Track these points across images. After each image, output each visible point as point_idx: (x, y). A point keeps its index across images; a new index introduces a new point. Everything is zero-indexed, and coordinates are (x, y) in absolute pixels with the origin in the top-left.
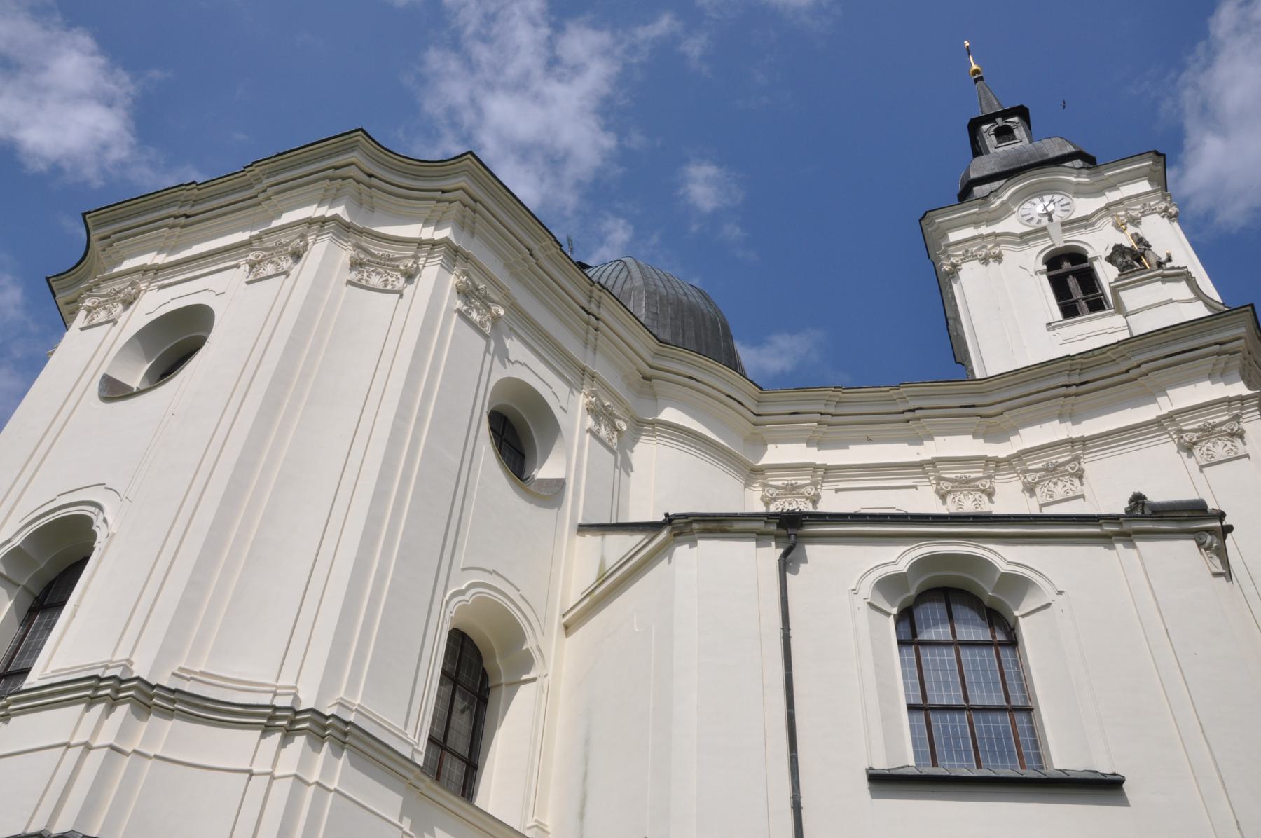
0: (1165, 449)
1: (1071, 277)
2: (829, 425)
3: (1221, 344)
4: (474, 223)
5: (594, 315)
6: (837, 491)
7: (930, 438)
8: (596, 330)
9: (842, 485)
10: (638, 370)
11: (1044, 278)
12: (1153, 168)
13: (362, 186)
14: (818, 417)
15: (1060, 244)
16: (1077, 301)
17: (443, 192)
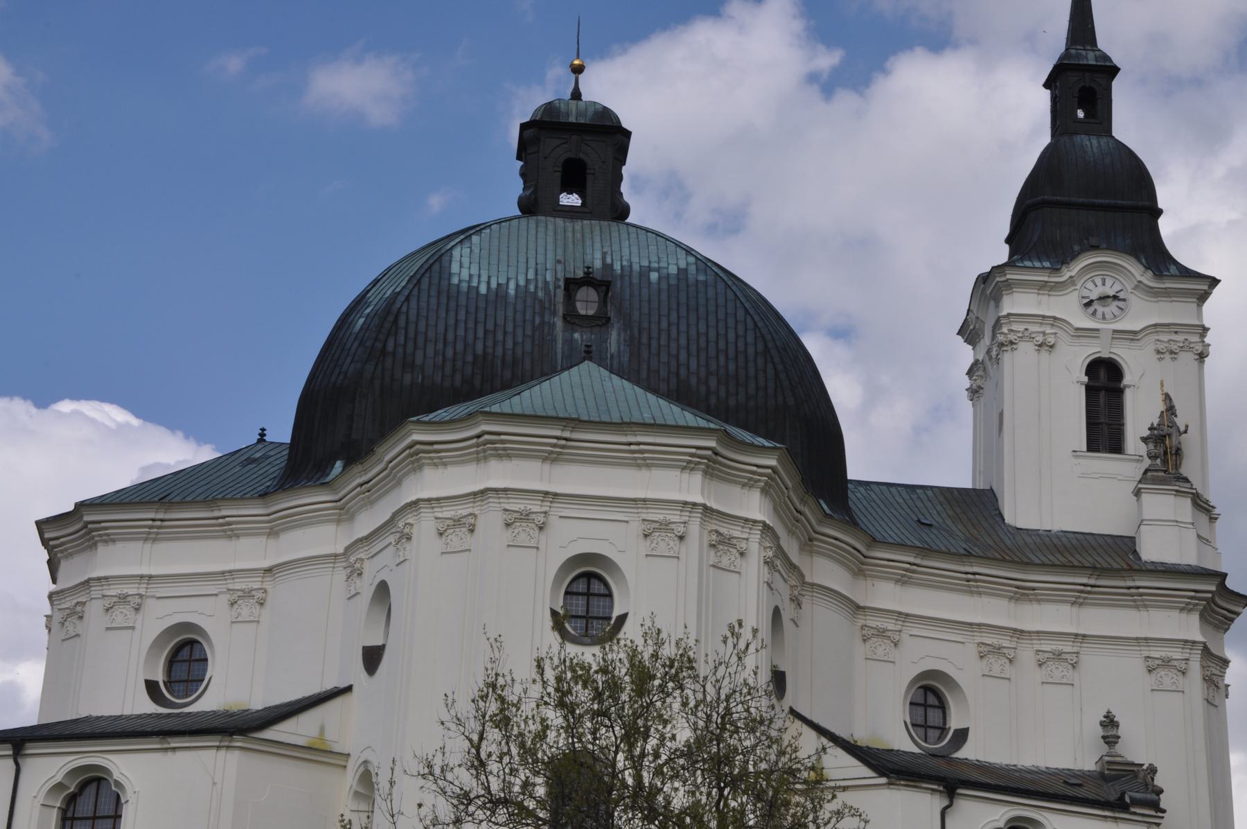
0: (1132, 663)
1: (1103, 392)
9: (915, 632)
11: (1083, 388)
15: (1105, 355)
16: (1101, 423)
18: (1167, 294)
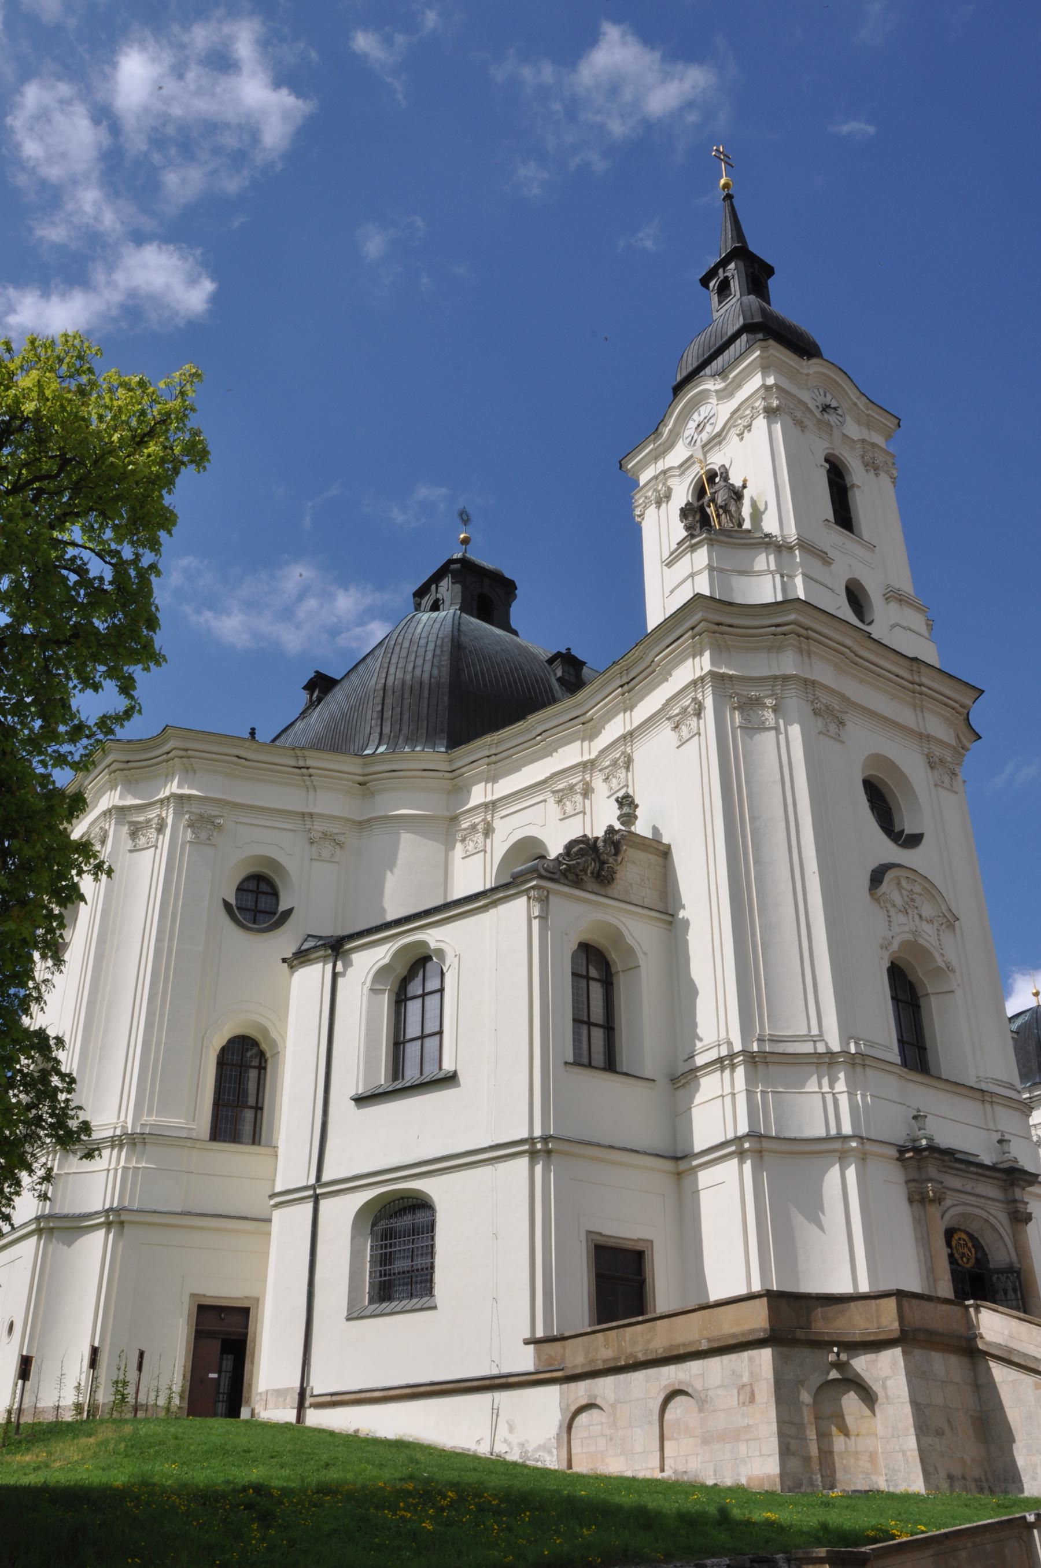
2: (495, 763)
3: (693, 628)
4: (192, 764)
5: (304, 768)
6: (502, 818)
7: (556, 750)
8: (310, 776)
9: (504, 813)
10: (354, 782)
12: (766, 355)
13: (125, 772)
14: (486, 760)
17: (168, 753)
18: (738, 385)
